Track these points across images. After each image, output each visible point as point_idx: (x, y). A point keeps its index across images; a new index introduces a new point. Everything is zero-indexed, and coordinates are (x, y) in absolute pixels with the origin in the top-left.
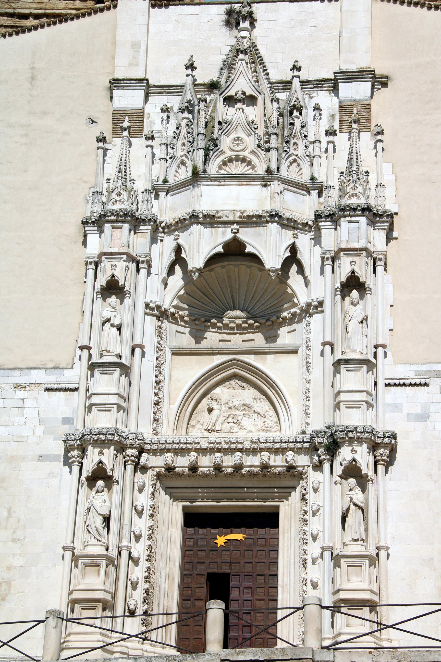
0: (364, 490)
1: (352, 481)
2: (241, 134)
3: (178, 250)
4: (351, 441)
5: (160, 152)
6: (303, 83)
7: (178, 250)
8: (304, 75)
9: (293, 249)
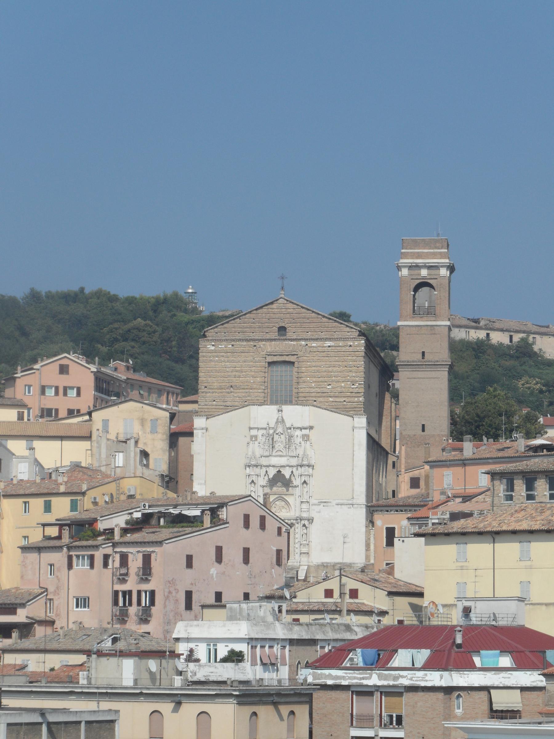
0: (307, 529)
1: (304, 528)
2: (280, 444)
3: (267, 472)
4: (304, 520)
5: (262, 446)
6: (294, 428)
7: (267, 472)
8: (294, 426)
9: (292, 472)
